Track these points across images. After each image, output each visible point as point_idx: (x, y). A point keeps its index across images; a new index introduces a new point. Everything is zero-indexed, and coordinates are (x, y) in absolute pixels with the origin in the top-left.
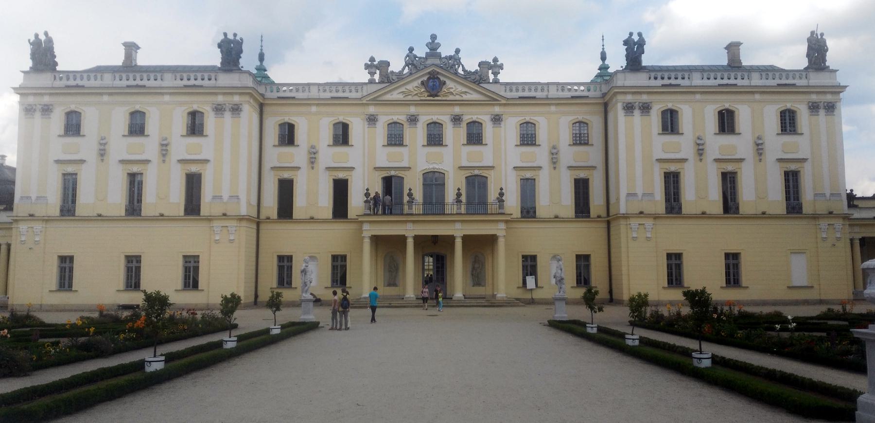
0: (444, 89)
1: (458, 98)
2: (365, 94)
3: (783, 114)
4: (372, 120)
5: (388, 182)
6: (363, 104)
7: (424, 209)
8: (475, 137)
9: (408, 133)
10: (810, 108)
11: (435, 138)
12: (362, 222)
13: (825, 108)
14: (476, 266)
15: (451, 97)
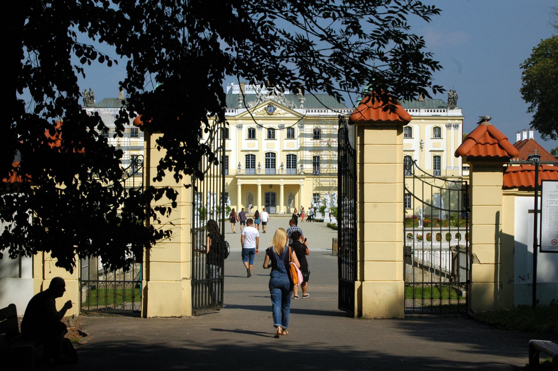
0: (275, 111)
1: (282, 116)
2: (237, 114)
3: (435, 128)
4: (240, 127)
5: (247, 156)
6: (236, 120)
7: (266, 172)
8: (291, 134)
9: (257, 132)
10: (446, 126)
11: (271, 134)
12: (237, 179)
13: (454, 126)
14: (291, 198)
15: (279, 116)
